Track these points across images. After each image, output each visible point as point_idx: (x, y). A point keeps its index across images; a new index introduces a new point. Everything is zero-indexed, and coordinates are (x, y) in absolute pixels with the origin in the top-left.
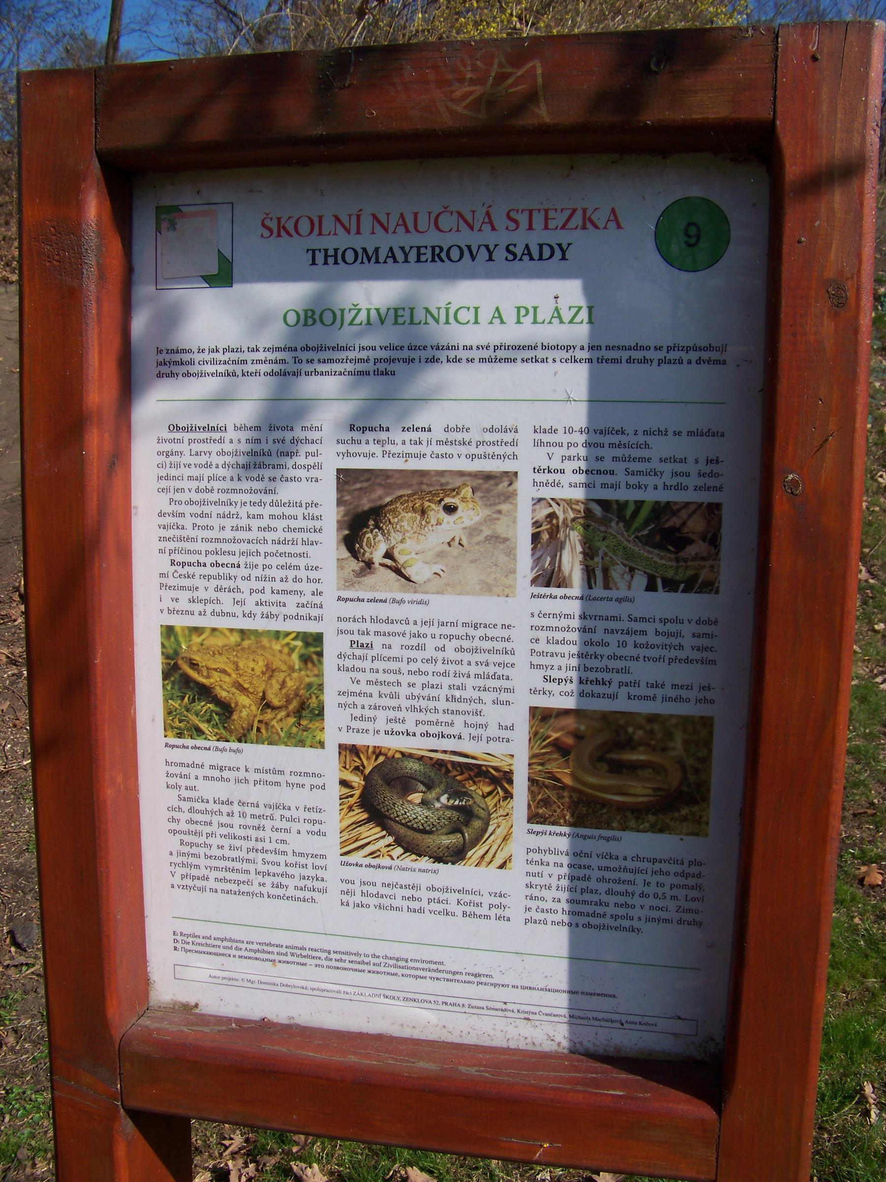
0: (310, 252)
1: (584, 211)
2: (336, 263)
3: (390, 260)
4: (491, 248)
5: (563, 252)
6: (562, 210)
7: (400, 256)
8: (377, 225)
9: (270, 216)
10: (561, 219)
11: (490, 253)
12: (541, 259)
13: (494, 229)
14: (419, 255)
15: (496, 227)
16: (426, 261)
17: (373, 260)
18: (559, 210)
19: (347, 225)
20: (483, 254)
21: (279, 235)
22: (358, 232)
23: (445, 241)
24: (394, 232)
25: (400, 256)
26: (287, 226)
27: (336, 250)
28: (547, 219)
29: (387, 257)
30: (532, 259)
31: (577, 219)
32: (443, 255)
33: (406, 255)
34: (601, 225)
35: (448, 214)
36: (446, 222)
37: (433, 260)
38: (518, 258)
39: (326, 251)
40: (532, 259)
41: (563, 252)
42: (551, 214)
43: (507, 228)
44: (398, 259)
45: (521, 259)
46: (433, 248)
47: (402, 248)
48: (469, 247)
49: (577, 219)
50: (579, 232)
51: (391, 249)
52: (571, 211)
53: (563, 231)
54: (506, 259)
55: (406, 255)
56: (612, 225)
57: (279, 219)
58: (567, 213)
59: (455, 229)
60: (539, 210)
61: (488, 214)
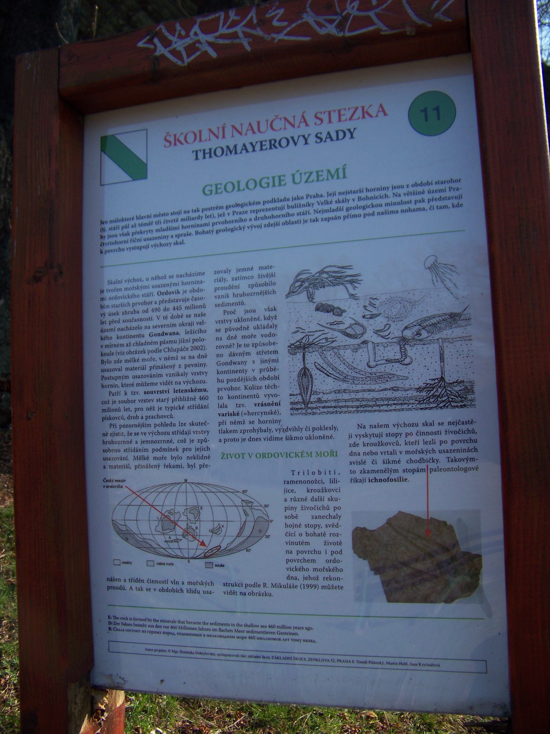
0: (195, 153)
1: (363, 108)
2: (210, 157)
3: (244, 152)
4: (306, 136)
6: (349, 109)
7: (250, 148)
9: (169, 134)
10: (348, 114)
11: (306, 140)
12: (338, 139)
13: (307, 125)
14: (262, 146)
15: (309, 123)
16: (266, 149)
17: (234, 152)
18: (347, 110)
19: (217, 134)
20: (302, 141)
21: (175, 144)
23: (277, 136)
24: (246, 134)
25: (250, 148)
27: (210, 150)
28: (340, 116)
29: (242, 149)
30: (332, 140)
32: (277, 144)
33: (254, 147)
34: (374, 114)
35: (279, 120)
36: (278, 124)
37: (271, 148)
38: (324, 140)
39: (204, 150)
40: (332, 140)
42: (342, 112)
43: (316, 124)
44: (249, 150)
46: (270, 141)
47: (251, 144)
48: (292, 138)
49: (359, 113)
52: (353, 110)
53: (351, 122)
54: (316, 142)
55: (254, 147)
56: (381, 114)
57: (175, 136)
58: (352, 111)
59: (283, 127)
60: (335, 111)
61: (303, 117)
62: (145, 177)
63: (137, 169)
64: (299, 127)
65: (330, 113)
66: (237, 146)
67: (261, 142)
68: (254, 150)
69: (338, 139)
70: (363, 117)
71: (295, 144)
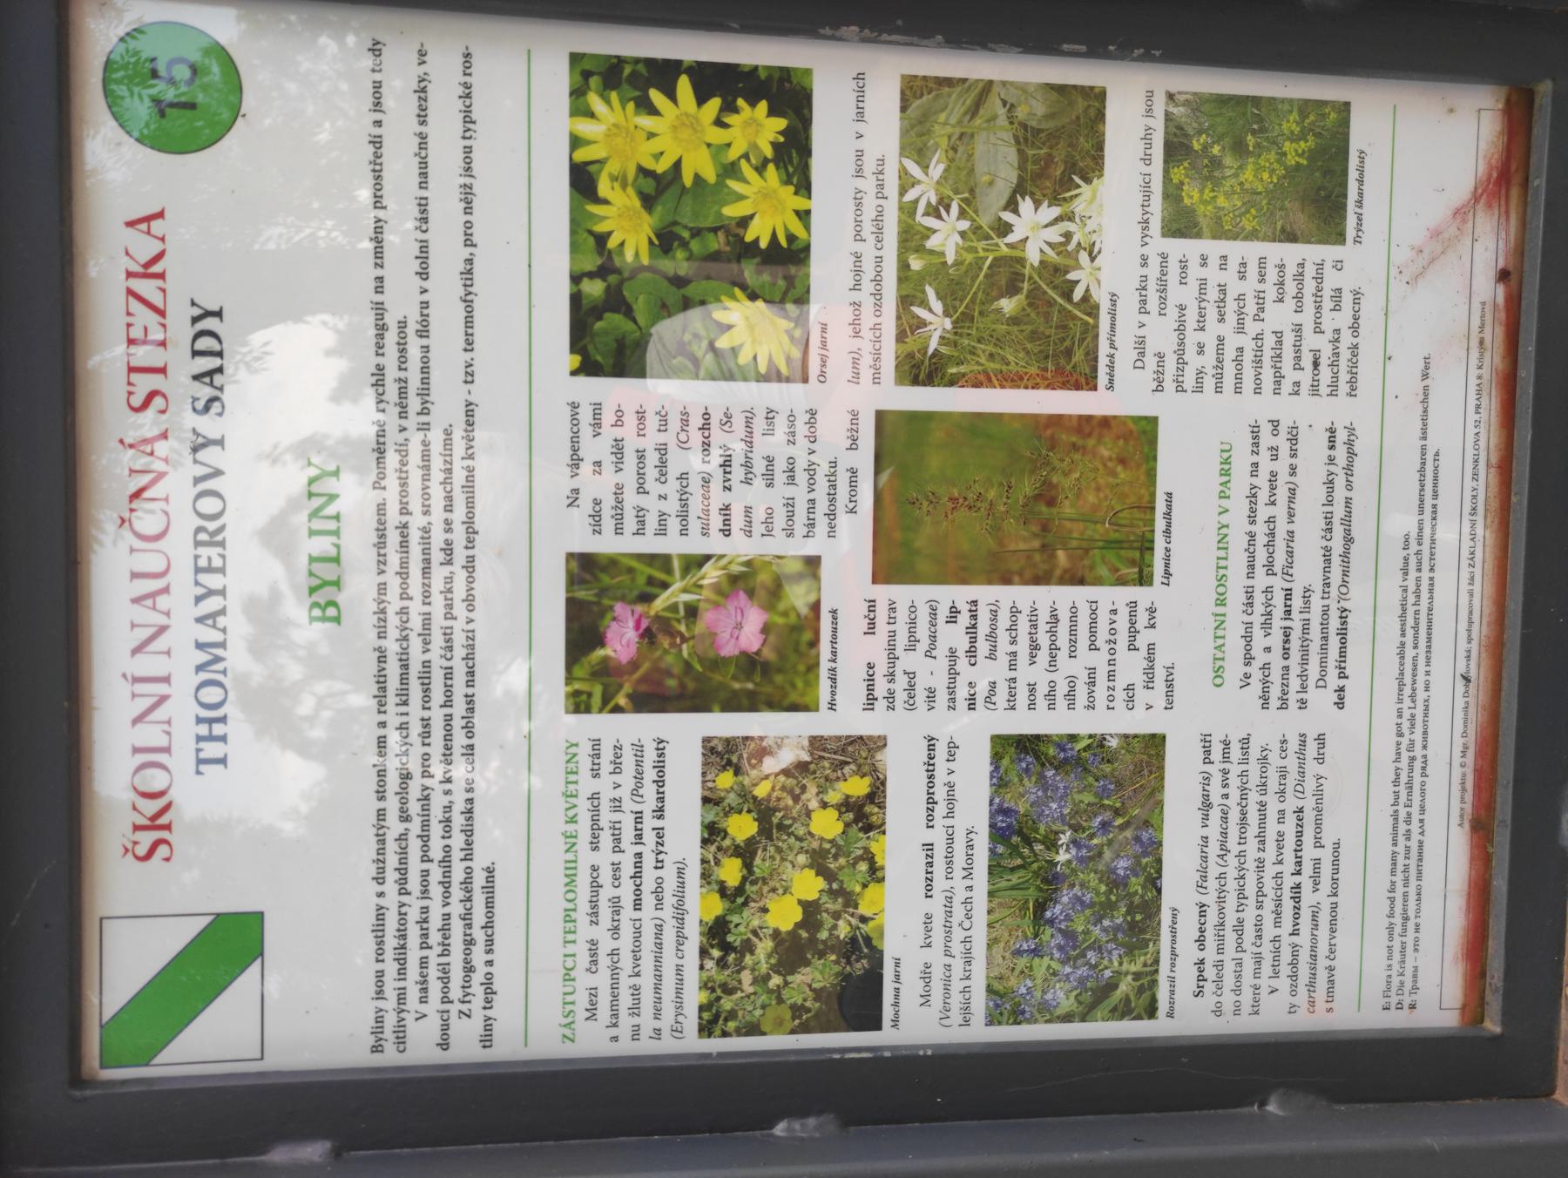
0: (203, 768)
1: (130, 275)
2: (223, 720)
3: (221, 621)
5: (208, 314)
6: (129, 314)
7: (212, 604)
8: (153, 647)
9: (130, 846)
10: (144, 316)
12: (220, 354)
14: (209, 570)
16: (223, 557)
17: (219, 652)
18: (130, 320)
19: (151, 701)
20: (210, 455)
21: (168, 827)
22: (166, 680)
23: (185, 524)
24: (168, 614)
25: (212, 604)
26: (150, 813)
27: (199, 720)
30: (220, 370)
31: (146, 288)
32: (212, 526)
33: (211, 593)
34: (158, 247)
37: (222, 544)
39: (199, 739)
40: (220, 370)
41: (208, 314)
46: (197, 544)
48: (197, 481)
49: (146, 288)
50: (169, 285)
51: (200, 620)
52: (131, 299)
54: (220, 414)
55: (211, 593)
56: (156, 226)
57: (137, 828)
58: (135, 306)
62: (262, 913)
63: (231, 944)
65: (132, 370)
66: (201, 640)
68: (222, 592)
70: (161, 276)
71: (218, 473)
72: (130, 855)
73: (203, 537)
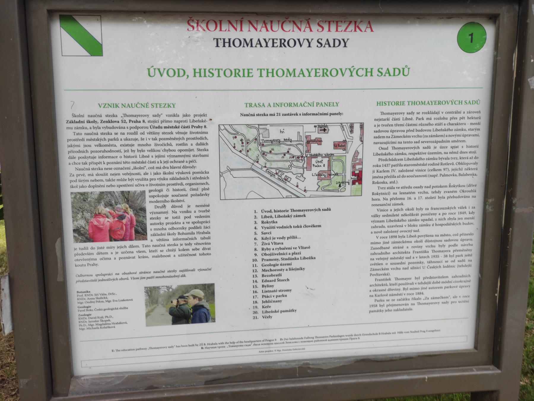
2: (230, 46)
3: (259, 46)
4: (310, 40)
5: (345, 44)
7: (264, 44)
12: (334, 46)
13: (311, 31)
14: (273, 43)
17: (250, 45)
20: (306, 44)
25: (264, 44)
27: (229, 40)
30: (330, 46)
32: (286, 44)
34: (363, 29)
37: (281, 46)
39: (224, 39)
40: (330, 46)
41: (345, 44)
45: (324, 47)
46: (281, 40)
47: (265, 40)
48: (299, 40)
50: (353, 32)
53: (345, 32)
64: (304, 31)
66: (253, 40)
67: (273, 40)
68: (267, 46)
69: (334, 46)
70: (355, 31)
71: (301, 46)
72: (189, 19)
73: (283, 41)
